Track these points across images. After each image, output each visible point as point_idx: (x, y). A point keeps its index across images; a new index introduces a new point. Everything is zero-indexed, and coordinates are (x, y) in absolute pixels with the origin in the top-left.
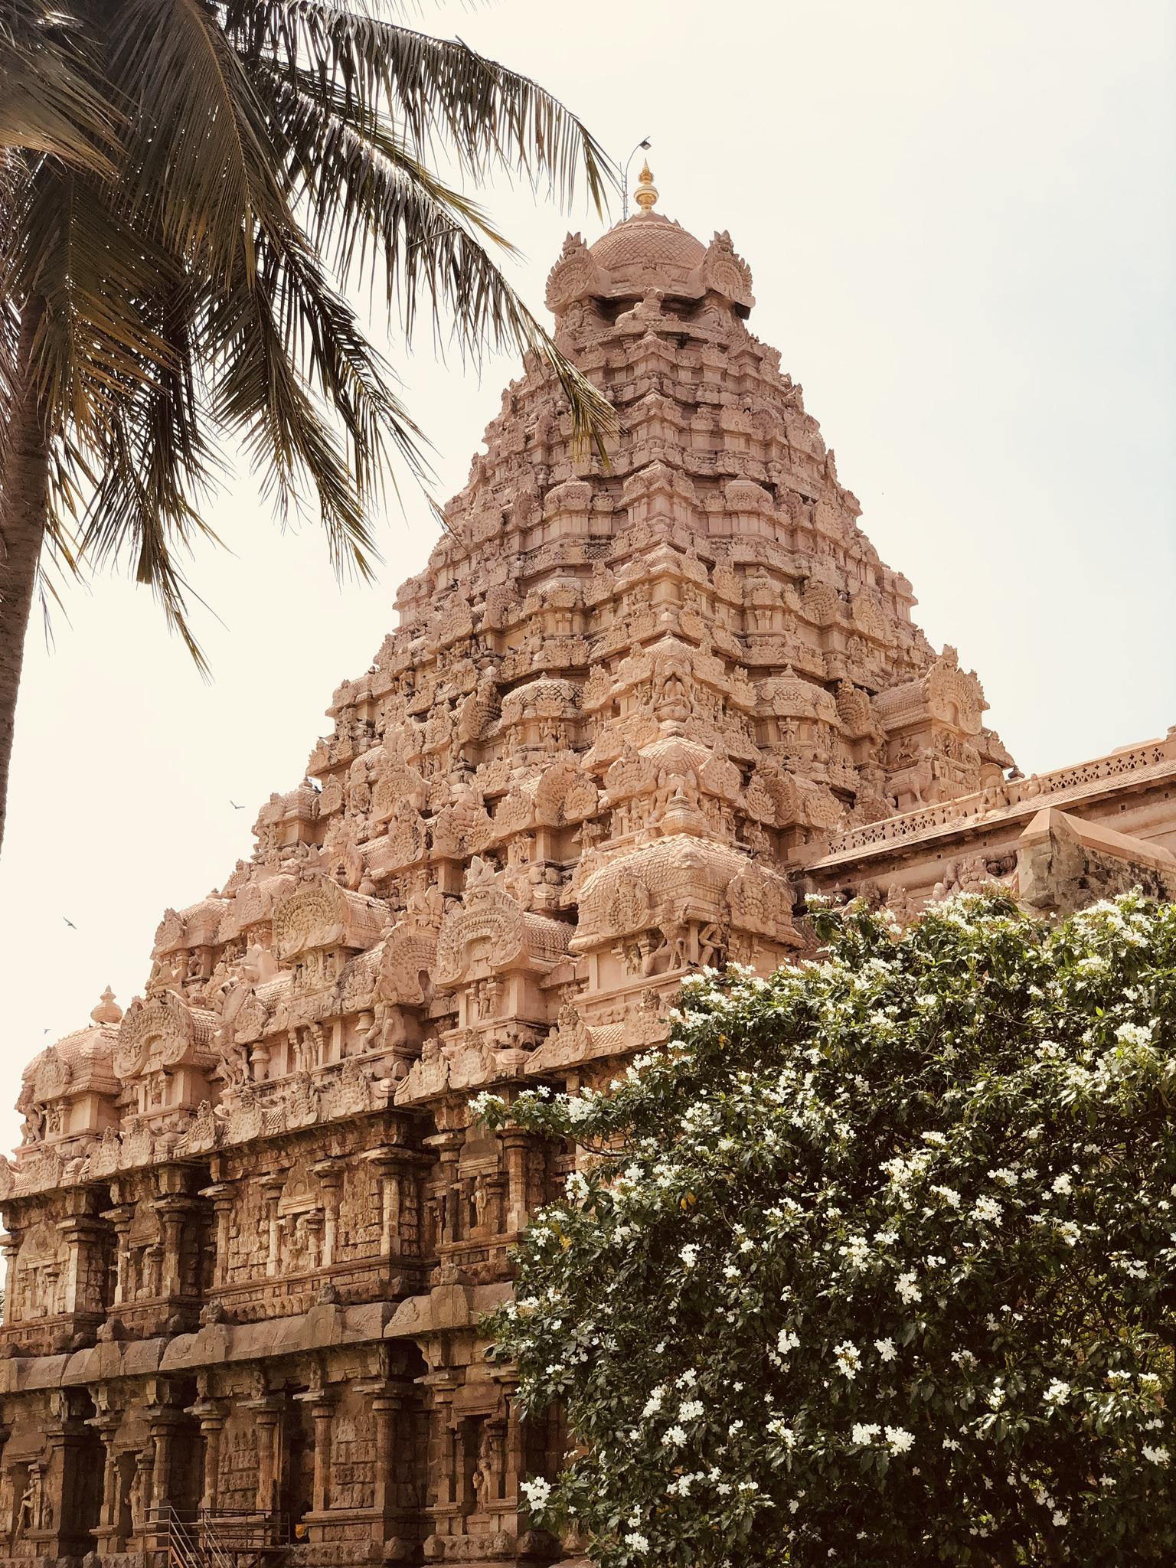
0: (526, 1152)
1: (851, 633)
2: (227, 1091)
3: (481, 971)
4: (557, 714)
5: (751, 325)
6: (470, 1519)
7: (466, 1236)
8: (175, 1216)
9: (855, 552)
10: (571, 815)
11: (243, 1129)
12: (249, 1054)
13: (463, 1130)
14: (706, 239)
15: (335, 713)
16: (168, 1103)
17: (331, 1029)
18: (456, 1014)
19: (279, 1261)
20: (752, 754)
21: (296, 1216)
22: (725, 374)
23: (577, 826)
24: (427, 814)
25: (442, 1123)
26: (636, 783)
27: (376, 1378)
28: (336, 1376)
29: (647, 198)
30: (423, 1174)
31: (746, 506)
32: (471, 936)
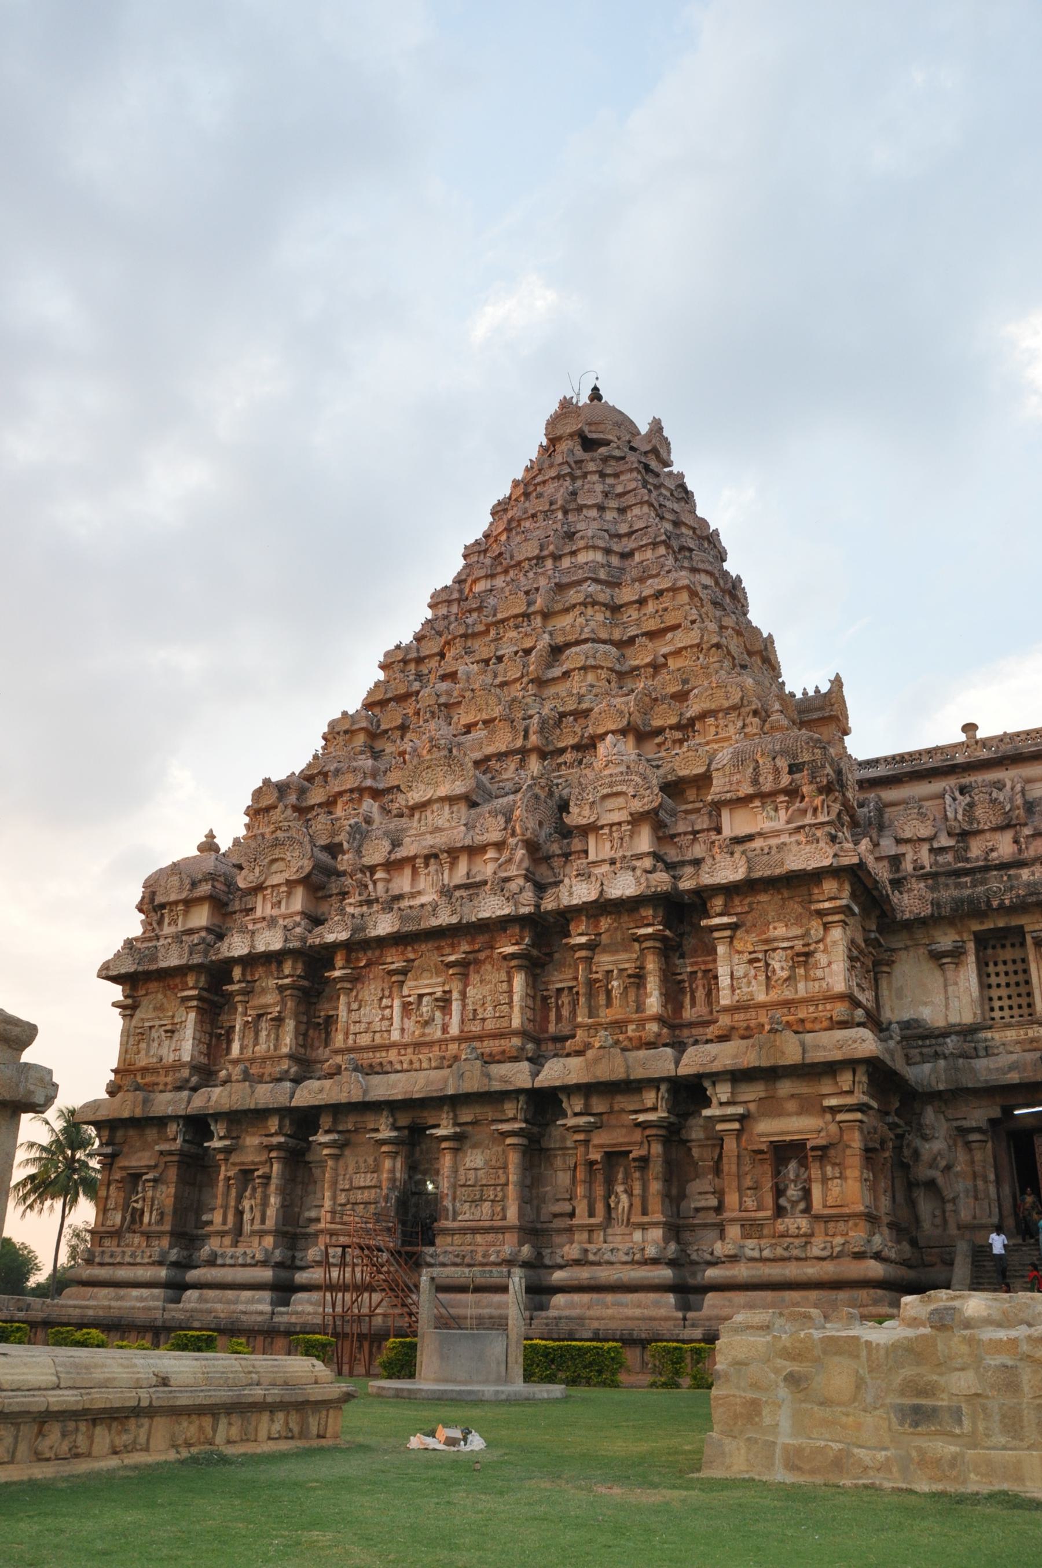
2: (351, 901)
3: (616, 817)
4: (610, 665)
6: (610, 1231)
7: (601, 1015)
8: (296, 992)
10: (657, 723)
11: (384, 925)
12: (372, 874)
13: (600, 934)
16: (287, 908)
19: (403, 1030)
21: (421, 996)
23: (659, 731)
26: (724, 702)
27: (514, 1119)
29: (596, 395)
30: (538, 971)
32: (605, 791)
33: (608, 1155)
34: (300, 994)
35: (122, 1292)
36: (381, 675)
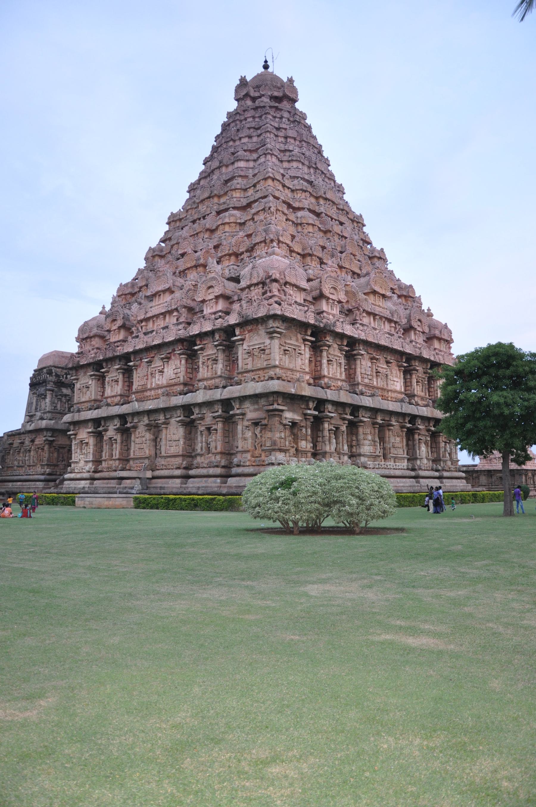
0: (224, 351)
1: (326, 199)
5: (297, 105)
9: (328, 175)
14: (285, 80)
15: (168, 223)
17: (165, 316)
18: (203, 311)
20: (295, 233)
22: (289, 120)
24: (196, 252)
25: (198, 342)
27: (180, 416)
28: (168, 417)
29: (266, 67)
30: (194, 358)
31: (294, 159)
34: (124, 371)
35: (110, 481)
36: (167, 228)
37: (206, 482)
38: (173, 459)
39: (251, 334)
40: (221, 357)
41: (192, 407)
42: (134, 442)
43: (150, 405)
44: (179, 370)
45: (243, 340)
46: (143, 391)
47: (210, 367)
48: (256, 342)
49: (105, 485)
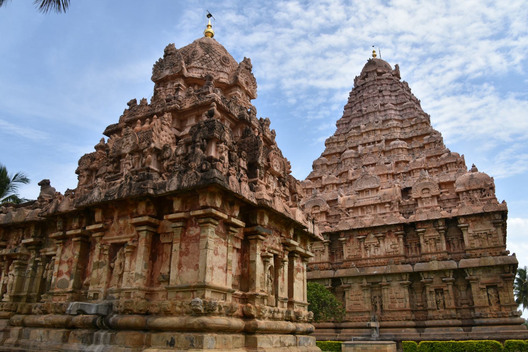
27: (406, 280)
29: (374, 56)
33: (435, 290)
37: (446, 330)
38: (399, 313)
39: (475, 223)
40: (443, 238)
41: (421, 274)
42: (348, 299)
43: (375, 271)
44: (397, 246)
45: (467, 227)
46: (358, 260)
47: (433, 245)
48: (481, 229)
49: (322, 334)
